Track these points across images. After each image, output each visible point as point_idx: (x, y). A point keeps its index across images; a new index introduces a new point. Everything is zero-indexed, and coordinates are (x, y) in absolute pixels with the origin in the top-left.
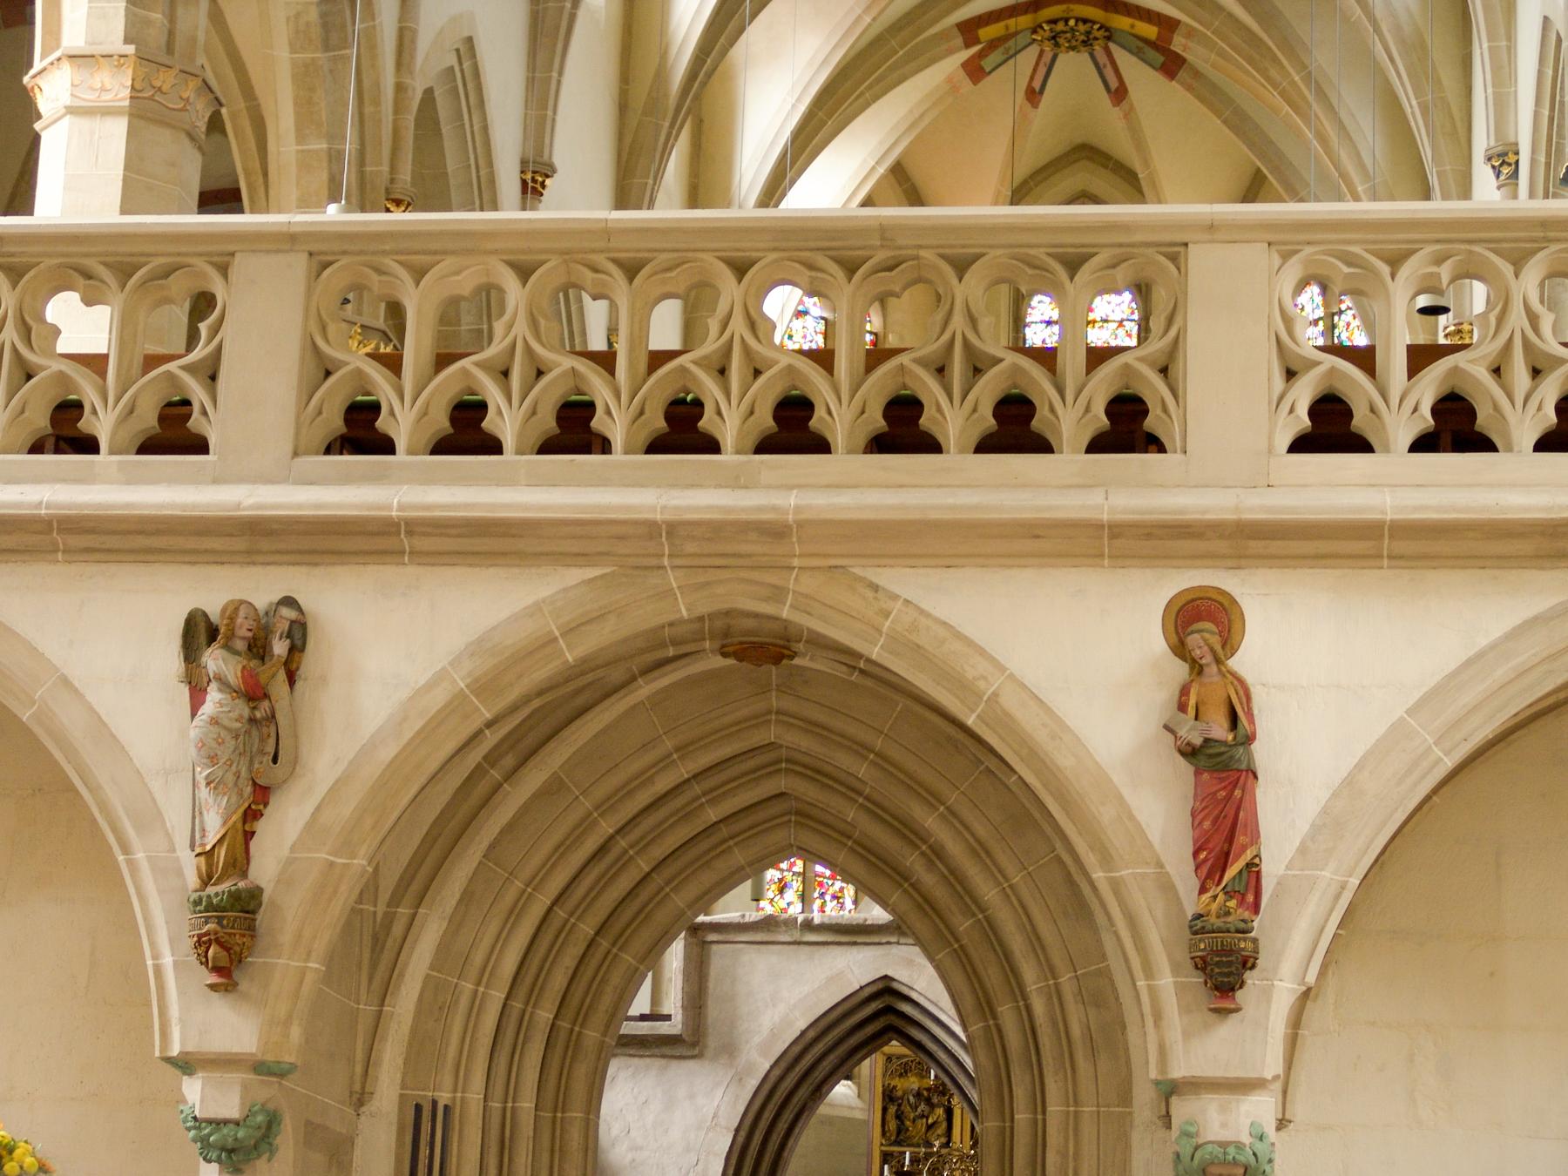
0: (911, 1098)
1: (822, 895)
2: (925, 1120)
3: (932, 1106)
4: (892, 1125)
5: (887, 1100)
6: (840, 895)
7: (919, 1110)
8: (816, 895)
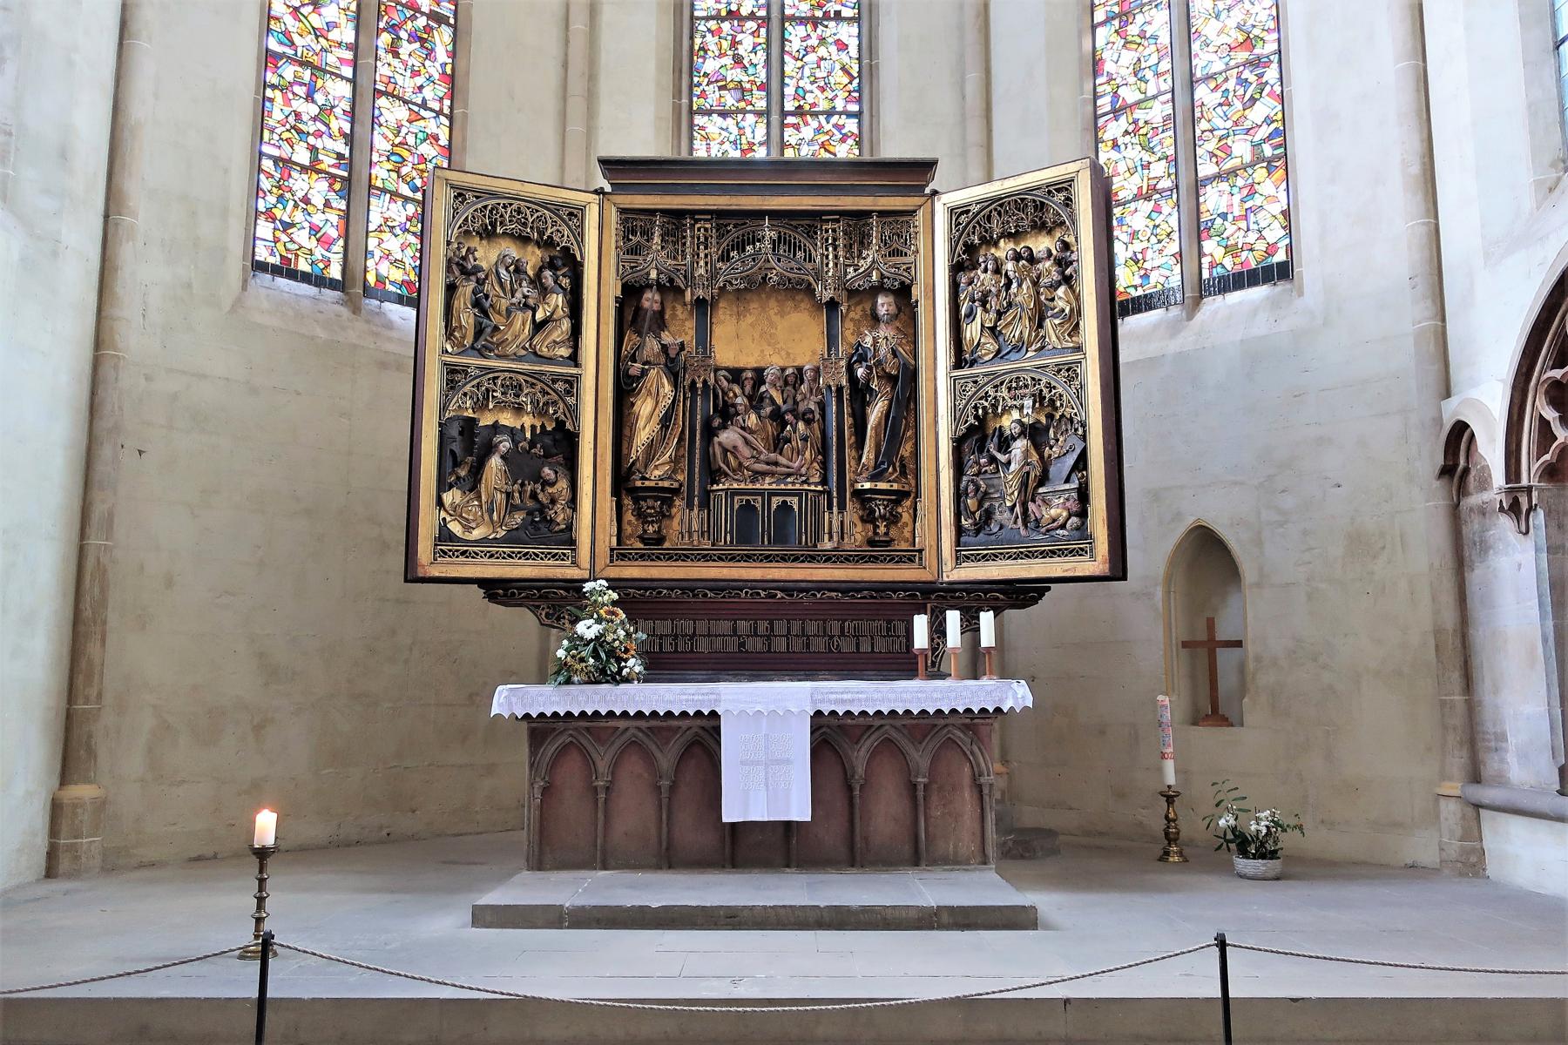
1: (393, 28)
3: (544, 292)
4: (467, 318)
6: (425, 36)
7: (518, 295)
8: (382, 25)
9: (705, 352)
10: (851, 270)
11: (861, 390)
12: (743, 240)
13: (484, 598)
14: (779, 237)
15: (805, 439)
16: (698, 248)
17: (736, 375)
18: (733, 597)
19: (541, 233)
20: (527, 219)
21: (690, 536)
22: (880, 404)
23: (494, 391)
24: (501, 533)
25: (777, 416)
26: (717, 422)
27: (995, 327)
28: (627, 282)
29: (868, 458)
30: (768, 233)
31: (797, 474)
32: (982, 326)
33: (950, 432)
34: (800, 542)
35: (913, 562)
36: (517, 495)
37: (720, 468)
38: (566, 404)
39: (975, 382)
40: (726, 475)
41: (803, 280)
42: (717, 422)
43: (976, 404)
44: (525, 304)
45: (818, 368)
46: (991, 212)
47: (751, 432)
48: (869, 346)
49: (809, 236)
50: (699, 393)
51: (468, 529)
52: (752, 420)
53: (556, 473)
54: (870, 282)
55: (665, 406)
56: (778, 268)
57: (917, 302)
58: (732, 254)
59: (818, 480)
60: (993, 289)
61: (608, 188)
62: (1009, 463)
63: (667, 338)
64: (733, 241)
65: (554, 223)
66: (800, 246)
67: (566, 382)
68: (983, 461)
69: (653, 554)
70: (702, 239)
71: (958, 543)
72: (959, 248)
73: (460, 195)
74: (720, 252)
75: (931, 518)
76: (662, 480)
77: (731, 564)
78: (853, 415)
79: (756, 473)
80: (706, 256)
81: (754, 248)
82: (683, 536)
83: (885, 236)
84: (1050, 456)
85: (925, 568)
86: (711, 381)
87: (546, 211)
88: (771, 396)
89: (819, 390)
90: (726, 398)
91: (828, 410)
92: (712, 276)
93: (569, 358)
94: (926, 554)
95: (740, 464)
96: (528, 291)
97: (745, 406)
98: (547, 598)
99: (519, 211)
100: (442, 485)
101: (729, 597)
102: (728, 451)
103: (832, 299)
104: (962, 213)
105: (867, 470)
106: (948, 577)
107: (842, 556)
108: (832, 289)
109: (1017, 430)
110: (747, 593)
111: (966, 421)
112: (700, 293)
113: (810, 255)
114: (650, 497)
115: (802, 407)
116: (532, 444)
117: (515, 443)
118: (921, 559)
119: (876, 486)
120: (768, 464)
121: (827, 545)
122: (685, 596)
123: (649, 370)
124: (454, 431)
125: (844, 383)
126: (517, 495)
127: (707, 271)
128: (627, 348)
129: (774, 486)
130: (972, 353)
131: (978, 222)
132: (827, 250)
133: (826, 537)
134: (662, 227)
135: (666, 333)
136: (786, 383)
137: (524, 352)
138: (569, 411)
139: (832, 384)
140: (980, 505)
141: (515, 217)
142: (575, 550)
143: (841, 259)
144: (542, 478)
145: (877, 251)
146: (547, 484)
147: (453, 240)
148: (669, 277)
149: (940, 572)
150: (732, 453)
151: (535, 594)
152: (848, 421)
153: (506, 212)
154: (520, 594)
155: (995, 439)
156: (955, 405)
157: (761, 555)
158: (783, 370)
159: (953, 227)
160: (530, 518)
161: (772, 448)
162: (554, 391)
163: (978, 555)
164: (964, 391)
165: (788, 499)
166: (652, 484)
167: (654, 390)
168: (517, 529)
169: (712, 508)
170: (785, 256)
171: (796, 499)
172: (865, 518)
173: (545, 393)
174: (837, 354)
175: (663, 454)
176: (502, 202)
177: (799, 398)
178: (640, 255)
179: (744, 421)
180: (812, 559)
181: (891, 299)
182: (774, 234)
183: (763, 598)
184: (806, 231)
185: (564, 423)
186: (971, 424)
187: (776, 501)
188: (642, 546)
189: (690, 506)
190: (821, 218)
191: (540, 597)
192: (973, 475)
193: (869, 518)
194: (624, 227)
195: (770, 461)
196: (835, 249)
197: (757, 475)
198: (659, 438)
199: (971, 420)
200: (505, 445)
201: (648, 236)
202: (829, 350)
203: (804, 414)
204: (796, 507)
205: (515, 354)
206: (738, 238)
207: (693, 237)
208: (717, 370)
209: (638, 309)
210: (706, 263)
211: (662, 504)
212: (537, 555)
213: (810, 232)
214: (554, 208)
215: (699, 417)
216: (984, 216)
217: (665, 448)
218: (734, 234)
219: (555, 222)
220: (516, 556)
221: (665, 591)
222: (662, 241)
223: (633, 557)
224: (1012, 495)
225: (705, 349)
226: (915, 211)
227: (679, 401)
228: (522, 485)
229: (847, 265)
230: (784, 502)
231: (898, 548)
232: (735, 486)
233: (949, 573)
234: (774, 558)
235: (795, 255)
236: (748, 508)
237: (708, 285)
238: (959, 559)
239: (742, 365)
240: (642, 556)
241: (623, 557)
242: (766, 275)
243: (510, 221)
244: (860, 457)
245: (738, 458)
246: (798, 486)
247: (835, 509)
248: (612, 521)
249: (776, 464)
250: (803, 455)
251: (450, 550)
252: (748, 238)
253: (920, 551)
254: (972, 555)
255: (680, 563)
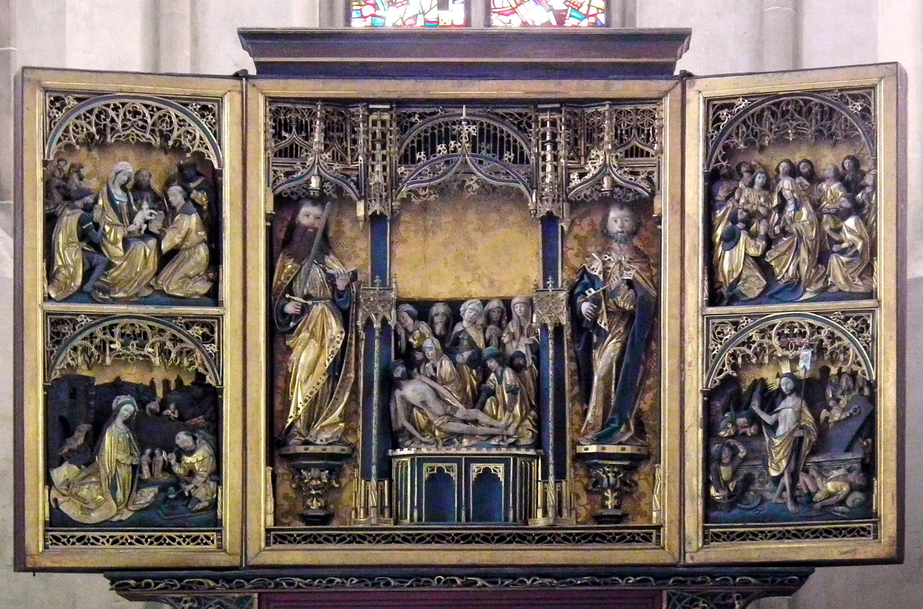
0: (119, 194)
2: (152, 242)
3: (170, 213)
5: (57, 197)
7: (139, 219)
9: (383, 284)
10: (574, 176)
11: (586, 329)
12: (433, 134)
13: (111, 589)
14: (481, 131)
15: (512, 391)
16: (374, 148)
17: (422, 309)
18: (423, 586)
19: (165, 137)
20: (146, 122)
21: (367, 513)
22: (610, 347)
23: (112, 342)
24: (126, 515)
25: (478, 362)
26: (399, 371)
27: (764, 255)
28: (280, 194)
29: (594, 415)
30: (466, 128)
31: (504, 436)
32: (746, 254)
33: (700, 385)
34: (507, 519)
35: (650, 542)
36: (146, 469)
37: (404, 428)
38: (203, 352)
39: (736, 324)
40: (411, 436)
41: (512, 188)
42: (399, 371)
43: (735, 351)
44: (147, 231)
45: (531, 300)
46: (763, 111)
47: (444, 383)
48: (596, 274)
49: (519, 128)
50: (377, 334)
51: (86, 510)
52: (446, 367)
53: (195, 438)
54: (600, 191)
55: (332, 352)
56: (479, 174)
57: (659, 218)
58: (418, 156)
59: (529, 442)
60: (761, 210)
61: (253, 71)
62: (776, 424)
63: (334, 266)
64: (419, 136)
65: (181, 123)
66: (508, 142)
67: (203, 325)
68: (741, 421)
69: (320, 535)
70: (379, 136)
71: (706, 519)
72: (717, 151)
73: (57, 100)
74: (402, 151)
75: (672, 487)
76: (330, 444)
77: (420, 546)
78: (575, 359)
79: (453, 434)
80: (384, 158)
81: (448, 148)
82: (356, 511)
83: (621, 130)
84: (827, 418)
85: (663, 548)
86: (392, 322)
87: (170, 109)
88: (470, 337)
89: (531, 330)
90: (411, 340)
91: (543, 353)
92: (392, 185)
93: (207, 295)
94: (665, 531)
95: (430, 422)
96: (151, 214)
97: (437, 350)
98: (191, 588)
99: (136, 113)
100: (52, 461)
101: (418, 586)
102: (413, 406)
103: (550, 214)
104: (722, 107)
105: (593, 429)
106: (692, 558)
107: (559, 535)
108: (550, 200)
109: (786, 385)
110: (439, 580)
111: (721, 372)
112: (376, 207)
113: (522, 153)
114: (315, 466)
115: (511, 349)
116: (164, 405)
117: (142, 404)
118: (658, 537)
119: (604, 449)
120: (465, 422)
121: (540, 520)
122: (362, 585)
123: (311, 306)
124: (64, 396)
125: (564, 320)
126: (146, 469)
127: (385, 178)
128: (280, 278)
129: (473, 451)
130: (733, 286)
131: (744, 122)
132: (544, 148)
133: (540, 513)
134: (325, 119)
135: (332, 257)
136: (489, 320)
137: (148, 292)
138: (209, 363)
139: (548, 321)
140: (735, 474)
141: (130, 120)
142: (220, 531)
143: (562, 160)
144: (177, 445)
145: (610, 151)
146: (181, 453)
147: (51, 158)
148: (337, 185)
149: (682, 552)
150: (419, 409)
151: (175, 585)
152: (569, 366)
153: (118, 116)
154: (156, 584)
155: (756, 394)
156: (708, 349)
157: (457, 535)
158: (485, 302)
159: (711, 122)
160: (163, 495)
161: (471, 403)
162: (187, 337)
163: (732, 533)
164: (719, 333)
165: (491, 466)
166: (318, 450)
167: (318, 333)
168: (147, 508)
169: (394, 477)
170: (487, 159)
171: (501, 467)
172: (590, 487)
173: (175, 340)
174: (555, 285)
175: (331, 412)
176: (112, 102)
177: (506, 339)
178: (296, 157)
179: (435, 369)
180: (522, 539)
181: (625, 213)
182: (473, 130)
183: (459, 587)
184: (516, 122)
185: (204, 376)
186: (728, 376)
187: (475, 468)
188: (303, 526)
189: (366, 476)
190: (536, 107)
191: (182, 588)
192: (729, 437)
193: (595, 488)
194: (275, 121)
195: (469, 418)
196: (555, 147)
197: (451, 438)
198: (326, 391)
199: (728, 370)
200: (126, 407)
201: (306, 131)
202: (545, 279)
203: (512, 359)
204: (501, 476)
205: (137, 294)
206: (426, 131)
207: (366, 132)
208: (400, 302)
209: (292, 227)
210: (384, 168)
211: (330, 473)
212: (173, 540)
213: (521, 123)
214: (184, 102)
215: (376, 365)
216: (753, 115)
217: (333, 404)
218: (420, 126)
219: (184, 121)
220: (146, 541)
221: (338, 580)
222: (325, 138)
223: (295, 539)
224: (778, 464)
225: (383, 278)
226: (660, 99)
227: (351, 345)
228: (152, 455)
229: (569, 168)
230: (487, 470)
231: (631, 524)
232: (424, 450)
233: (693, 554)
234: (474, 538)
235: (501, 157)
236: (438, 480)
237: (387, 198)
238: (708, 538)
239: (430, 296)
240: (305, 539)
241: (281, 539)
242: (464, 182)
243: (124, 126)
244: (585, 413)
245: (426, 415)
246: (503, 450)
247: (551, 479)
248: (266, 495)
249: (476, 422)
250: (511, 411)
251: (64, 537)
252: (440, 131)
253: (658, 528)
254: (724, 533)
255: (355, 546)
